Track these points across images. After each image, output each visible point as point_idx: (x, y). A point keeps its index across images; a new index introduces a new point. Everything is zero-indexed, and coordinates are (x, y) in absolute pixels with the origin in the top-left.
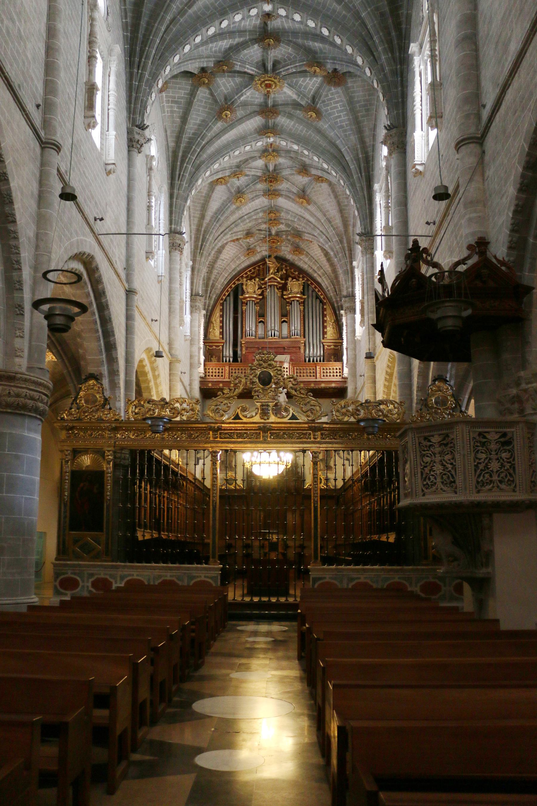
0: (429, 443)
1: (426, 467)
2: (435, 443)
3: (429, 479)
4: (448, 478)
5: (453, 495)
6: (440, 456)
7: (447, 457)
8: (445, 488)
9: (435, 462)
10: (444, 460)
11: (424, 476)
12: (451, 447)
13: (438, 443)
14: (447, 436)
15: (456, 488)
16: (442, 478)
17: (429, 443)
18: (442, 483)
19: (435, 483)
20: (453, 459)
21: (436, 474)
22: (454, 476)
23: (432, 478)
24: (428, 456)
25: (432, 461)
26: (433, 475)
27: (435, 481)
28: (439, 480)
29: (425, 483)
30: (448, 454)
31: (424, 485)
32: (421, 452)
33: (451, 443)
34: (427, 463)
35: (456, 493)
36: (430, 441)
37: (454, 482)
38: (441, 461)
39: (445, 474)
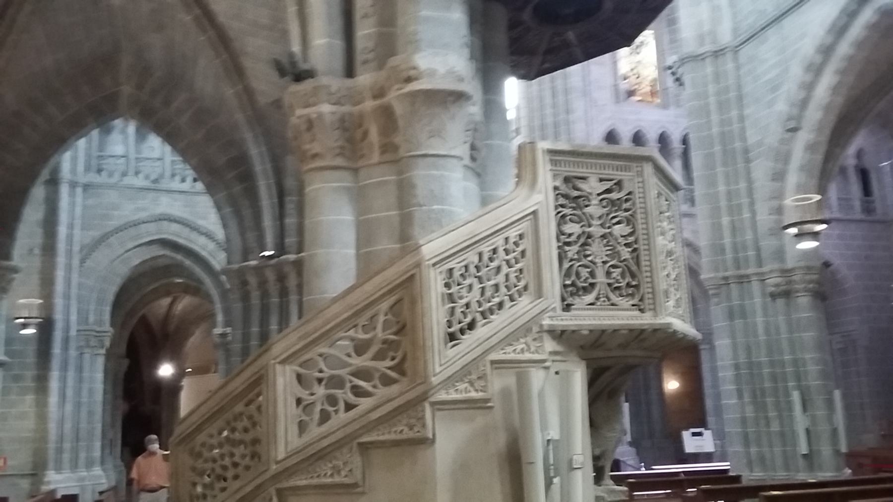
1: (568, 244)
3: (578, 275)
4: (623, 275)
6: (602, 225)
7: (619, 230)
8: (614, 298)
11: (566, 265)
12: (626, 210)
13: (599, 195)
14: (619, 184)
16: (608, 274)
17: (576, 193)
18: (609, 285)
19: (592, 285)
20: (631, 234)
22: (637, 273)
23: (584, 273)
25: (584, 233)
27: (591, 281)
28: (601, 278)
29: (568, 282)
30: (618, 223)
31: (565, 286)
33: (627, 200)
35: (642, 311)
37: (637, 287)
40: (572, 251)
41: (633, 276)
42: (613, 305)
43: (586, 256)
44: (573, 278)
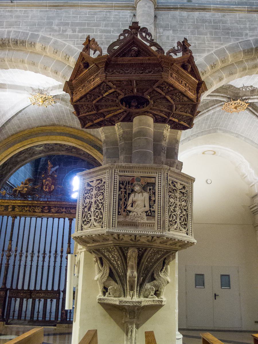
0: (174, 188)
1: (170, 206)
2: (177, 189)
3: (173, 217)
5: (186, 235)
9: (176, 204)
10: (181, 205)
11: (170, 214)
13: (179, 190)
14: (184, 187)
15: (187, 230)
16: (180, 219)
17: (174, 188)
18: (180, 223)
20: (186, 206)
21: (177, 214)
23: (175, 217)
24: (172, 197)
25: (174, 203)
26: (175, 215)
30: (183, 201)
32: (168, 192)
34: (172, 203)
36: (174, 186)
38: (180, 205)
39: (181, 217)
40: (172, 208)
41: (186, 221)
42: (180, 230)
43: (175, 211)
44: (171, 218)
